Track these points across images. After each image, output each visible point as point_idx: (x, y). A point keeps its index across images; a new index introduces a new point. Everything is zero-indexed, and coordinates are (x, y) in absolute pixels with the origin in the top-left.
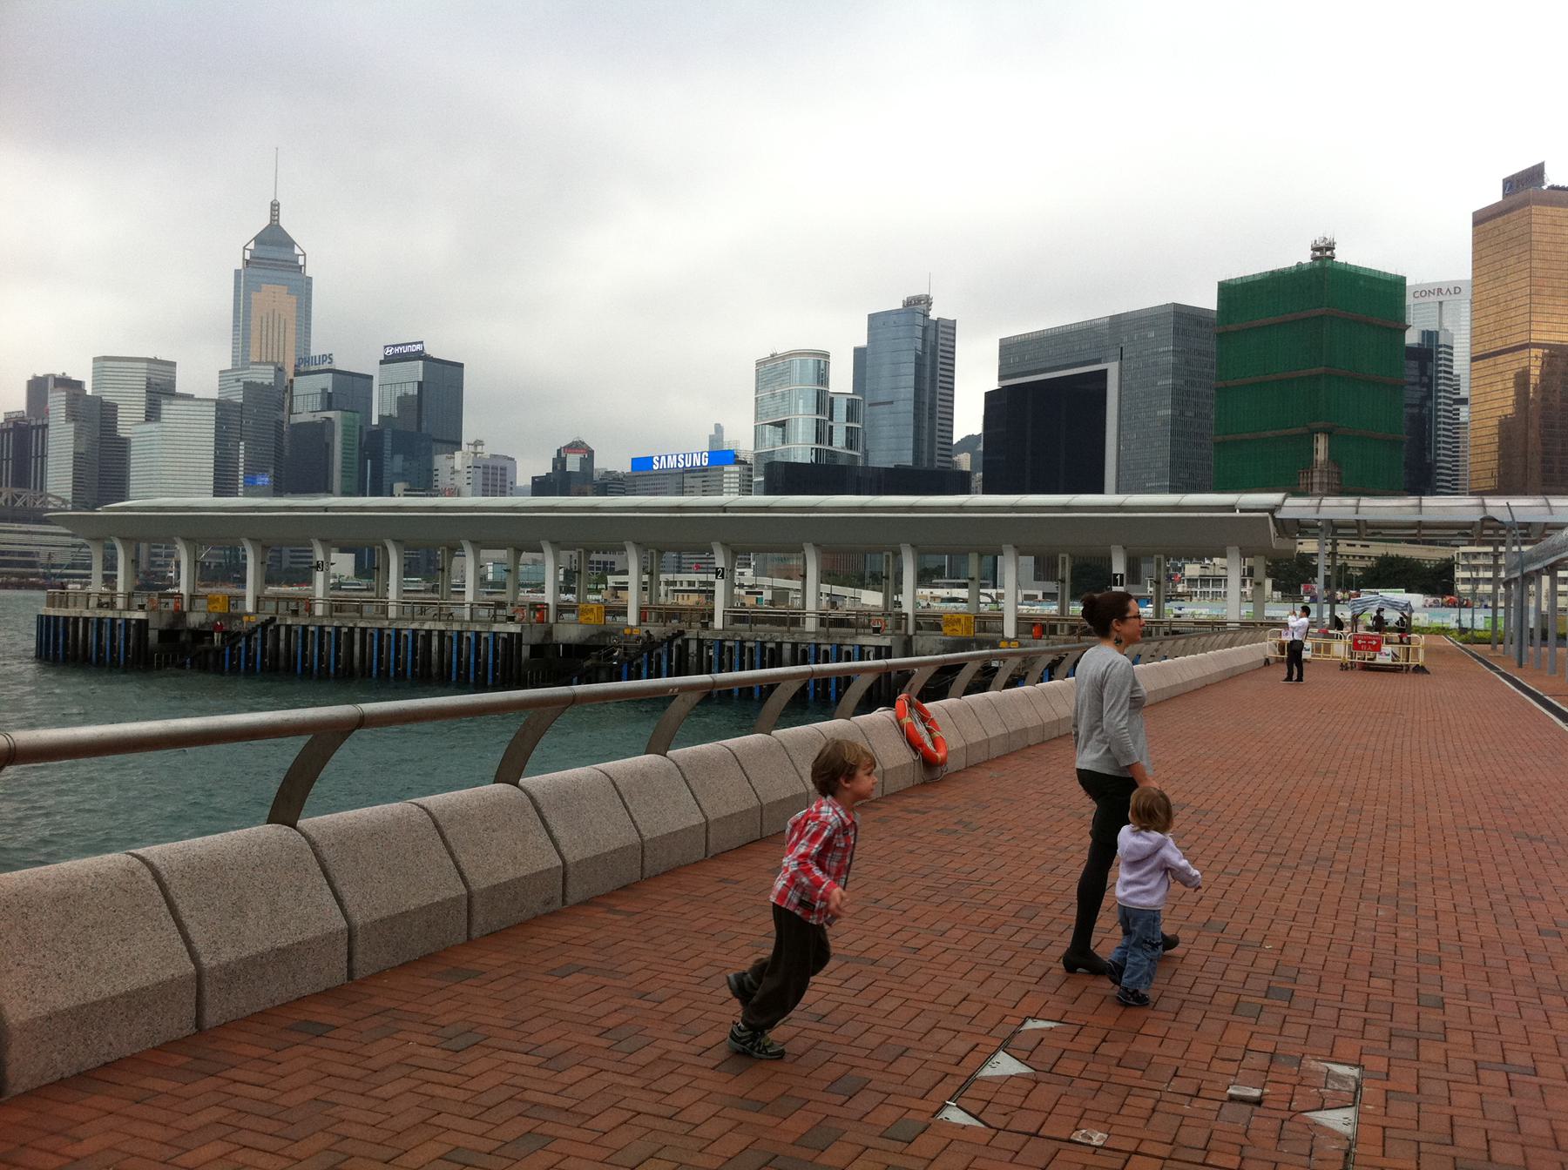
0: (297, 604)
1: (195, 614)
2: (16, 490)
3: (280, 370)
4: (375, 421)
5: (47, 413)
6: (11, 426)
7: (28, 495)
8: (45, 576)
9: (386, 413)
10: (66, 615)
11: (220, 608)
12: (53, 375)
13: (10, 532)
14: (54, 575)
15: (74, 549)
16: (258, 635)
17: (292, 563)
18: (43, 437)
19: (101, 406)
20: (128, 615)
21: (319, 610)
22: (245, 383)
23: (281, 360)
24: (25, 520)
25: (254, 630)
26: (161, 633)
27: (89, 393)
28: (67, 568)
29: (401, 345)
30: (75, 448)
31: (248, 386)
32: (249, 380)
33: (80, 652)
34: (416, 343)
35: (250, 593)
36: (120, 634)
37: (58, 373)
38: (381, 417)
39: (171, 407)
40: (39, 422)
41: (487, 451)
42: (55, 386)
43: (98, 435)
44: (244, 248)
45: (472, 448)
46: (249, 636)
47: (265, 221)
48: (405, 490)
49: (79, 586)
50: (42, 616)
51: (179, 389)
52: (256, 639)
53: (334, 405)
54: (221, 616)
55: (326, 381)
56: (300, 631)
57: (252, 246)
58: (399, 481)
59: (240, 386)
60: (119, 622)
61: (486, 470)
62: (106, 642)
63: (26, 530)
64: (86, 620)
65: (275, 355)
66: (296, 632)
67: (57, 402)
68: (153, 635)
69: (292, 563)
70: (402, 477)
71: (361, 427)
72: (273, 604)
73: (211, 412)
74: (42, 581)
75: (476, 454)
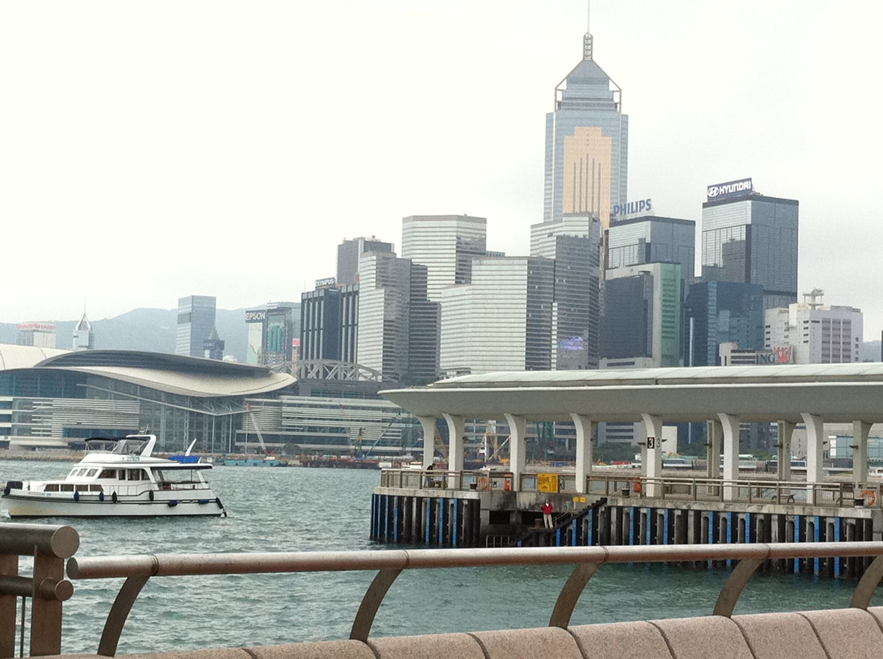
0: (628, 484)
1: (525, 494)
2: (327, 362)
3: (595, 221)
4: (698, 273)
5: (358, 280)
6: (322, 294)
7: (339, 367)
8: (356, 454)
9: (711, 263)
10: (401, 494)
11: (551, 488)
12: (363, 238)
13: (321, 406)
14: (365, 452)
15: (385, 424)
16: (589, 517)
17: (608, 437)
18: (354, 304)
19: (412, 269)
20: (461, 495)
21: (650, 491)
22: (558, 237)
23: (596, 210)
24: (338, 395)
25: (586, 513)
26: (492, 513)
27: (399, 256)
28: (377, 445)
29: (726, 184)
30: (385, 316)
31: (562, 240)
32: (562, 234)
33: (414, 533)
34: (743, 181)
35: (579, 470)
36: (453, 515)
37: (368, 237)
38: (705, 268)
39: (482, 268)
40: (350, 289)
41: (827, 302)
42: (365, 251)
43: (408, 300)
44: (556, 89)
45: (809, 300)
46: (580, 518)
47: (580, 58)
48: (733, 351)
49: (390, 464)
50: (377, 496)
51: (490, 247)
52: (587, 521)
53: (652, 258)
54: (551, 497)
55: (643, 230)
56: (632, 514)
57: (564, 86)
58: (725, 341)
59: (553, 241)
60: (451, 502)
61: (826, 325)
62: (439, 523)
63: (337, 404)
64: (420, 500)
65: (590, 205)
66: (628, 514)
67: (367, 266)
68: (484, 516)
69: (608, 437)
70: (728, 336)
71: (682, 281)
72: (603, 484)
73: (522, 272)
74: (353, 459)
75: (814, 306)
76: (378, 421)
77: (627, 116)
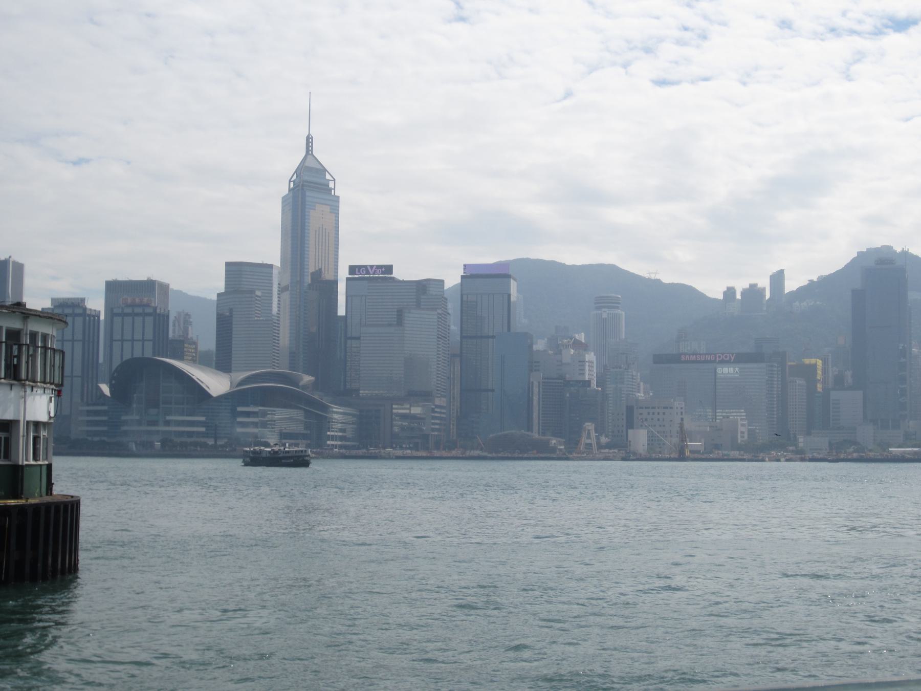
76: (349, 424)
77: (338, 197)
